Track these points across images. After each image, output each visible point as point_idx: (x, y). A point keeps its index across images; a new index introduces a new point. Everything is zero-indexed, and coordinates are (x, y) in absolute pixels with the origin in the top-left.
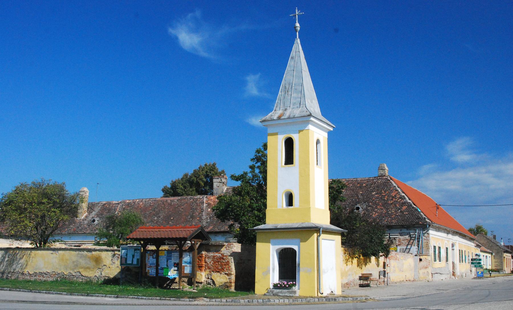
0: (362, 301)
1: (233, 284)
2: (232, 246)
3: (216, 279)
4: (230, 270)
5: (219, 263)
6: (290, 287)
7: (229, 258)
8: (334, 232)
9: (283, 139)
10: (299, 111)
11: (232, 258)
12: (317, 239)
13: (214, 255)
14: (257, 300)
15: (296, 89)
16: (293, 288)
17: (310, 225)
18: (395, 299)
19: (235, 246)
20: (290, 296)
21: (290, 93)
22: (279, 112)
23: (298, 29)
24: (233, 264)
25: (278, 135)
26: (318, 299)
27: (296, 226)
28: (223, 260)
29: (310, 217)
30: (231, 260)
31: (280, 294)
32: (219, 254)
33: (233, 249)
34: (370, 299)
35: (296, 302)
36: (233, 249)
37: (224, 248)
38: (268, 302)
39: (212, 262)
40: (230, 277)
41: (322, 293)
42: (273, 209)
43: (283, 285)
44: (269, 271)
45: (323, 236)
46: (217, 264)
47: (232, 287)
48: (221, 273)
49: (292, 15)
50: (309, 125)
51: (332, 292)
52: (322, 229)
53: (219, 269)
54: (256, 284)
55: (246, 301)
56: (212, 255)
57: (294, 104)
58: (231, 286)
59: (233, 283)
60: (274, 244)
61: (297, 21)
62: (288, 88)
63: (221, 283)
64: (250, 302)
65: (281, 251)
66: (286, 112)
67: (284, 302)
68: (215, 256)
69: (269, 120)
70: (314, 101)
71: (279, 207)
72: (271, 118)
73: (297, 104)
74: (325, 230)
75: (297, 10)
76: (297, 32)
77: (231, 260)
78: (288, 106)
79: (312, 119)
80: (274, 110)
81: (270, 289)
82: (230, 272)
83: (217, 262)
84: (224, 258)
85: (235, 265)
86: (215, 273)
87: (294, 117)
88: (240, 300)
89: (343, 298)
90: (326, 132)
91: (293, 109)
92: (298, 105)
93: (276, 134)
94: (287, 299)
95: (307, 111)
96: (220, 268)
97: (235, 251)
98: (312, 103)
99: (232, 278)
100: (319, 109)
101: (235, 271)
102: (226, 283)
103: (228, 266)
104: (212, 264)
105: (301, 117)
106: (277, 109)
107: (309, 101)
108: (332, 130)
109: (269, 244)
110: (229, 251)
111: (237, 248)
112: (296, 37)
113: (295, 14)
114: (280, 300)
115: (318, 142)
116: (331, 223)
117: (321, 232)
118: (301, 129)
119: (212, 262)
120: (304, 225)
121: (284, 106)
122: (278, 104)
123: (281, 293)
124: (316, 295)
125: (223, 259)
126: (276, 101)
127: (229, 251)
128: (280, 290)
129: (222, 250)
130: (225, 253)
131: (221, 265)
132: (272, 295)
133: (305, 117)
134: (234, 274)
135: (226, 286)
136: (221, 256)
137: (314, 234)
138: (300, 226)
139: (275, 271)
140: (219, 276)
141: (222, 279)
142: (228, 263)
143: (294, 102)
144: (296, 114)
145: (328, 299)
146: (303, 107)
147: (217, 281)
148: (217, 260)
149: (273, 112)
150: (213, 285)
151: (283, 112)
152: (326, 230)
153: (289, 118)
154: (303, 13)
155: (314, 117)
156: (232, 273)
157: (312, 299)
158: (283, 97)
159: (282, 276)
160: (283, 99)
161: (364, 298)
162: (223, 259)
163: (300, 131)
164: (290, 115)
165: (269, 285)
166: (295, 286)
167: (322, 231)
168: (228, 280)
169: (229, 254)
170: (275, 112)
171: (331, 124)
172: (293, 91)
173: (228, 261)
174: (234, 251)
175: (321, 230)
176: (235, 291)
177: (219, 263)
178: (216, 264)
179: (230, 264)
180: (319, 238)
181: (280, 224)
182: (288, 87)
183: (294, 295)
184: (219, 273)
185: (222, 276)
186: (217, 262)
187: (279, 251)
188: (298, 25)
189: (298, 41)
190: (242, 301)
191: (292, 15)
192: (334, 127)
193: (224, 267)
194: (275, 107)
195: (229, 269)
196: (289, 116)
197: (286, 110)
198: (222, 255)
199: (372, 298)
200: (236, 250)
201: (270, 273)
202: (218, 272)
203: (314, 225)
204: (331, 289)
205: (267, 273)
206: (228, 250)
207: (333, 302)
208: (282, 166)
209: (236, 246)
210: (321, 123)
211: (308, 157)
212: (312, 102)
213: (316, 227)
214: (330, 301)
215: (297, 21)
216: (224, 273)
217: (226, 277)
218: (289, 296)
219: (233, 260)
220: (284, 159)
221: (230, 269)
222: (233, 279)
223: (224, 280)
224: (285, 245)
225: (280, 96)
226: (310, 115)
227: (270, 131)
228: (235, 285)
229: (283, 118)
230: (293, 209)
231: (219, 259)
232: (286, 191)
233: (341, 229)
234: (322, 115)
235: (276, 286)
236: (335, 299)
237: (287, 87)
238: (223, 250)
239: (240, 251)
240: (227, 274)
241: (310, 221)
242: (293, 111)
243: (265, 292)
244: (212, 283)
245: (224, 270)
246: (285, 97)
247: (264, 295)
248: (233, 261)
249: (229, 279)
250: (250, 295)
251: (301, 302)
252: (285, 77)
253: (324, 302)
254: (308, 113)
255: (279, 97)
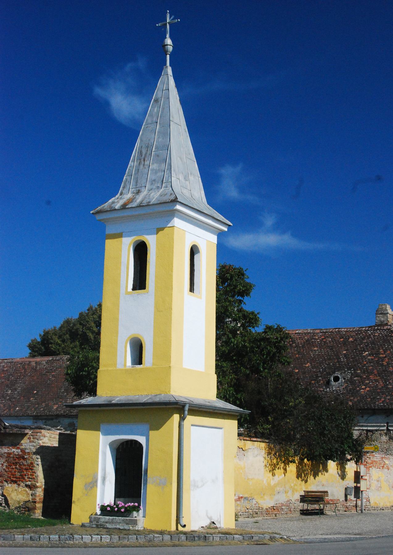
0: (259, 543)
1: (39, 505)
2: (40, 436)
3: (10, 494)
4: (34, 478)
5: (18, 466)
6: (128, 512)
7: (34, 456)
8: (221, 414)
9: (130, 244)
10: (158, 194)
11: (39, 457)
12: (180, 426)
13: (10, 451)
14: (47, 537)
15: (158, 156)
16: (133, 515)
17: (167, 399)
18: (321, 540)
19: (45, 437)
20: (119, 529)
21: (147, 163)
22: (128, 196)
23: (170, 48)
24: (40, 468)
25: (122, 237)
26: (171, 536)
27: (144, 400)
28: (23, 461)
29: (170, 384)
30: (37, 460)
31: (109, 526)
32: (17, 450)
33: (40, 442)
34: (281, 538)
35: (125, 542)
36: (40, 442)
37: (26, 438)
38: (70, 540)
39: (5, 464)
40: (33, 492)
41: (183, 525)
42: (110, 369)
43: (116, 509)
44: (96, 481)
45: (190, 419)
46: (14, 467)
47: (36, 511)
48: (19, 485)
49: (160, 25)
50: (174, 218)
51: (213, 523)
52: (189, 406)
53: (16, 478)
54: (73, 505)
55: (27, 536)
56: (6, 451)
57: (153, 182)
58: (35, 508)
59: (39, 502)
60: (106, 434)
61: (168, 36)
62: (146, 154)
63: (19, 502)
64: (34, 540)
65: (120, 445)
66: (137, 196)
67: (101, 540)
68: (10, 454)
69: (107, 211)
70: (191, 178)
71: (120, 366)
72: (110, 207)
73: (158, 182)
74: (212, 411)
75: (168, 16)
76: (167, 54)
77: (37, 460)
78: (143, 185)
79: (178, 207)
80: (119, 194)
81: (96, 514)
82: (34, 482)
83: (13, 463)
84: (25, 457)
85: (43, 470)
86: (10, 485)
87: (148, 205)
88: (16, 536)
89: (223, 535)
90: (214, 234)
91: (151, 192)
92: (159, 185)
93: (120, 235)
94: (107, 536)
95: (171, 194)
96: (18, 475)
97: (44, 445)
98: (186, 180)
99: (37, 494)
100: (203, 192)
101: (43, 481)
102: (26, 502)
103: (31, 471)
104: (5, 467)
105: (160, 203)
106: (124, 192)
107: (181, 177)
108: (226, 229)
109: (99, 432)
110: (35, 444)
111: (49, 440)
112: (165, 64)
113: (165, 23)
114: (94, 536)
115: (194, 251)
116: (219, 396)
117: (186, 412)
118: (162, 226)
119: (5, 464)
120: (157, 400)
121: (136, 185)
122: (127, 183)
123: (112, 522)
124: (173, 528)
125: (24, 459)
126: (125, 178)
127: (35, 444)
128: (110, 517)
129: (22, 442)
130: (28, 447)
131: (21, 470)
132: (94, 526)
133: (165, 205)
134: (41, 487)
135: (28, 508)
136: (21, 453)
137: (173, 415)
138: (150, 401)
139: (107, 483)
140: (16, 490)
141: (20, 495)
142: (31, 467)
143: (153, 178)
144: (152, 200)
145: (190, 537)
146: (167, 187)
147: (12, 498)
148: (13, 461)
149: (117, 196)
150: (5, 507)
151: (134, 196)
152: (215, 410)
153: (140, 206)
154: (179, 20)
155: (183, 204)
156: (38, 484)
157: (158, 537)
158: (135, 170)
159: (119, 493)
160: (135, 174)
161: (267, 537)
162: (24, 459)
163: (159, 230)
164: (142, 201)
165: (96, 510)
166: (138, 511)
167: (189, 410)
168: (30, 498)
169: (34, 451)
170: (120, 197)
171: (225, 219)
172: (153, 159)
173: (32, 463)
174: (42, 444)
175: (187, 408)
176: (42, 518)
177: (18, 466)
178: (13, 468)
179: (34, 468)
180: (182, 423)
181: (118, 397)
182: (145, 153)
183: (131, 528)
184: (16, 485)
185: (20, 490)
186: (13, 463)
187: (116, 446)
188: (169, 41)
189: (169, 70)
190: (19, 537)
191: (160, 25)
192: (229, 226)
193: (25, 472)
194: (121, 189)
195: (34, 478)
196: (141, 203)
197: (138, 192)
198: (23, 451)
199: (285, 537)
200: (47, 443)
201: (97, 486)
202: (15, 482)
203: (172, 400)
204: (210, 518)
205: (92, 485)
206: (34, 444)
207: (201, 543)
208: (127, 293)
209: (48, 435)
210: (192, 211)
211: (171, 276)
212: (186, 178)
213: (176, 403)
214: (195, 540)
215: (168, 36)
216: (24, 485)
217: (27, 491)
218: (122, 529)
219: (40, 460)
220: (133, 279)
221: (34, 476)
222: (39, 496)
223: (24, 498)
224: (122, 434)
225: (131, 168)
226: (175, 201)
227: (109, 230)
228: (43, 506)
229: (130, 206)
230: (142, 369)
231: (18, 458)
232: (133, 337)
233: (239, 409)
234: (208, 203)
235: (104, 510)
236: (206, 537)
237: (144, 152)
238: (25, 443)
239: (57, 445)
240: (29, 486)
241: (169, 391)
242: (149, 195)
243: (86, 521)
244: (3, 502)
245: (24, 479)
246: (138, 170)
247: (81, 527)
248: (40, 463)
249: (32, 495)
250: (59, 527)
251: (135, 541)
252: (142, 134)
253: (182, 541)
254: (172, 197)
255: (129, 169)
